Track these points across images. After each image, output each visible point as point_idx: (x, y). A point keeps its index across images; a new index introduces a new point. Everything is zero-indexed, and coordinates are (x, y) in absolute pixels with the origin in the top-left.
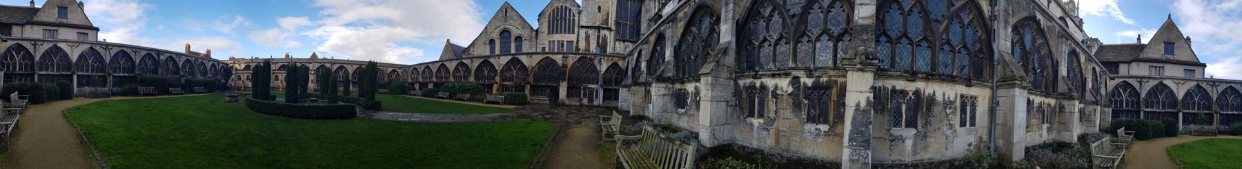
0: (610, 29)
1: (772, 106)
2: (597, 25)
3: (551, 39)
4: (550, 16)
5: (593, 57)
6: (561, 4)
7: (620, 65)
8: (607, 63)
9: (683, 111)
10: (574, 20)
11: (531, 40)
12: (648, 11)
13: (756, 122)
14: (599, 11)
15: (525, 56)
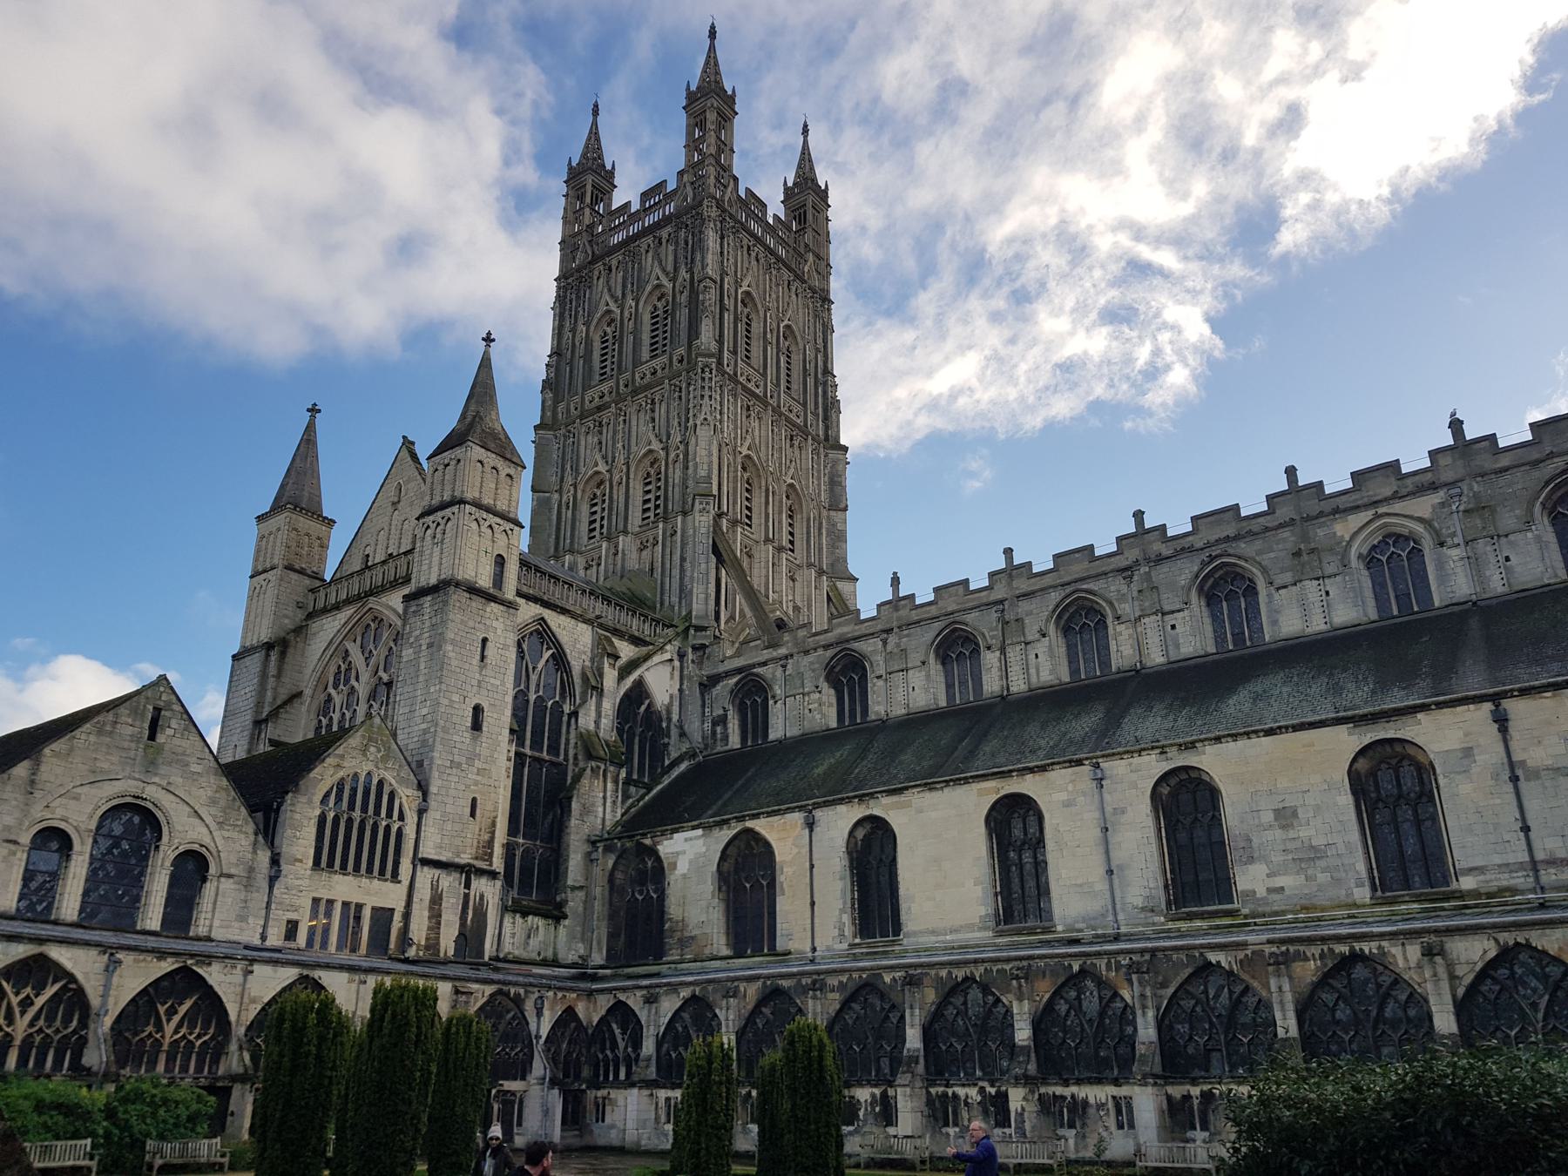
0: (493, 875)
1: (965, 1115)
2: (465, 859)
3: (325, 895)
4: (327, 795)
5: (522, 991)
6: (367, 767)
7: (581, 1016)
8: (552, 1009)
9: (851, 1128)
10: (400, 831)
11: (248, 883)
12: (586, 810)
13: (952, 1131)
14: (473, 814)
15: (344, 976)
